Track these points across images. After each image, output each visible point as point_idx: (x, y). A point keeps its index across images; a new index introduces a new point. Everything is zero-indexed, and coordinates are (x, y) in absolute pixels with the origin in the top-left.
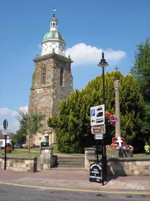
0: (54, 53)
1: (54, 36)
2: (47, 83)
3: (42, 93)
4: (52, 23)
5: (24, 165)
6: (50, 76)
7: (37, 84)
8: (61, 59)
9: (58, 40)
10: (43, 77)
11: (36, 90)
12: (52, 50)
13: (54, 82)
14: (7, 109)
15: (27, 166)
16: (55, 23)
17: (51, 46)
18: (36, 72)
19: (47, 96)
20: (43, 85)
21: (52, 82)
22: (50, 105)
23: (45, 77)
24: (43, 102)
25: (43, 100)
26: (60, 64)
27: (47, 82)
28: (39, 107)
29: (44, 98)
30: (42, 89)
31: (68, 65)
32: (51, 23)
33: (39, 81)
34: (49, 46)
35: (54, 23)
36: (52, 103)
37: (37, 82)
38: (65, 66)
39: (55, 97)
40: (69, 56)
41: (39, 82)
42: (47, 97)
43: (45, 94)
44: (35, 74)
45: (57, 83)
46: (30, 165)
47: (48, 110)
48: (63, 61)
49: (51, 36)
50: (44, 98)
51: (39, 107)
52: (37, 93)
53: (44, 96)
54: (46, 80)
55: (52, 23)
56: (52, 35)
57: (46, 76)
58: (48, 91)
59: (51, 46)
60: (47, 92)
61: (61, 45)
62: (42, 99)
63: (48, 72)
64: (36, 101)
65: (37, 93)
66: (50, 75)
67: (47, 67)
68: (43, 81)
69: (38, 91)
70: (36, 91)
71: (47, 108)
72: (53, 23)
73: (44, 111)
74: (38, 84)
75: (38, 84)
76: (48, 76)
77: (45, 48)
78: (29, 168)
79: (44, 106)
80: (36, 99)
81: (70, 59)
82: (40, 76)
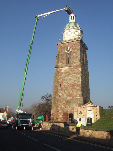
3: (68, 72)
4: (71, 17)
6: (77, 57)
7: (61, 64)
10: (68, 58)
11: (60, 69)
14: (81, 71)
17: (74, 33)
18: (60, 54)
19: (74, 74)
20: (69, 64)
22: (78, 82)
24: (70, 79)
25: (69, 77)
27: (73, 62)
29: (71, 76)
30: (68, 68)
32: (70, 16)
33: (64, 61)
34: (73, 33)
35: (73, 17)
37: (62, 62)
41: (64, 62)
42: (74, 75)
43: (71, 73)
44: (59, 55)
47: (76, 86)
50: (70, 76)
52: (62, 71)
53: (71, 74)
54: (72, 61)
55: (71, 17)
57: (72, 57)
58: (76, 70)
59: (74, 33)
63: (75, 53)
64: (61, 78)
65: (62, 71)
66: (77, 56)
68: (67, 61)
69: (63, 69)
70: (61, 70)
71: (75, 84)
73: (71, 88)
75: (63, 63)
77: (68, 35)
79: (71, 82)
80: (61, 77)
82: (64, 57)
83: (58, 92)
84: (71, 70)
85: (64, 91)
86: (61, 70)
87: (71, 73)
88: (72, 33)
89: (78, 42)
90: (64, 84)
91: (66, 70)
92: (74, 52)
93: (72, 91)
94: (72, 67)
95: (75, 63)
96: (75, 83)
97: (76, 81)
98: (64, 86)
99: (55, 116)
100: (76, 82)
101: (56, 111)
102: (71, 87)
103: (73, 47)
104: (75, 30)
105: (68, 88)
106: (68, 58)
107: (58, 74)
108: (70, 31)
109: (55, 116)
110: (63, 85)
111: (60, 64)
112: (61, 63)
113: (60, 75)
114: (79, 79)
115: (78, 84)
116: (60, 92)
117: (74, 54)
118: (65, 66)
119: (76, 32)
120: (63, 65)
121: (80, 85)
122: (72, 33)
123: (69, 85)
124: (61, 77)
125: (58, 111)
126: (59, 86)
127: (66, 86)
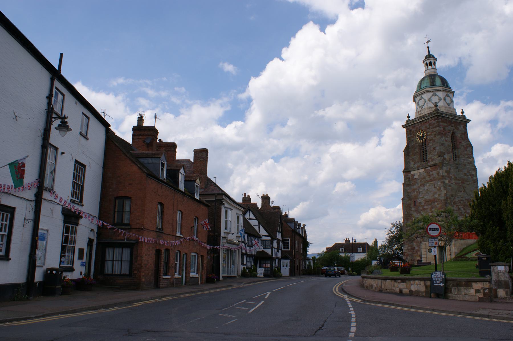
0: (438, 110)
1: (433, 84)
2: (430, 160)
3: (424, 178)
5: (472, 291)
7: (412, 163)
8: (450, 119)
9: (441, 88)
10: (423, 152)
11: (412, 173)
12: (433, 105)
13: (442, 158)
15: (477, 291)
16: (432, 61)
17: (430, 100)
21: (439, 158)
22: (439, 195)
23: (426, 151)
24: (427, 191)
25: (426, 188)
26: (450, 128)
27: (431, 158)
28: (420, 200)
30: (423, 170)
31: (462, 126)
33: (417, 158)
36: (444, 192)
38: (458, 129)
39: (447, 181)
40: (463, 112)
43: (429, 179)
45: (448, 159)
46: (482, 291)
47: (436, 203)
48: (454, 122)
49: (428, 84)
50: (428, 185)
51: (420, 200)
52: (415, 177)
53: (428, 181)
54: (429, 156)
56: (430, 82)
58: (434, 173)
60: (433, 174)
61: (447, 95)
62: (424, 186)
64: (414, 190)
65: (415, 177)
67: (428, 134)
69: (416, 173)
70: (414, 175)
72: (428, 62)
73: (429, 206)
74: (415, 163)
75: (415, 163)
76: (432, 149)
78: (481, 295)
79: (429, 197)
80: (414, 187)
81: (464, 117)
82: (417, 150)
83: (412, 215)
84: (428, 172)
85: (420, 213)
86: (414, 175)
87: (428, 178)
88: (425, 102)
89: (435, 120)
90: (420, 199)
91: (420, 174)
92: (430, 140)
93: (432, 212)
94: (429, 168)
95: (433, 160)
96: (435, 198)
97: (436, 193)
98: (420, 203)
99: (408, 257)
100: (436, 196)
101: (410, 248)
102: (430, 204)
103: (428, 130)
104: (431, 94)
105: (425, 207)
106: (423, 152)
107: (408, 183)
108: (422, 98)
109: (408, 257)
110: (418, 201)
111: (412, 164)
112: (413, 161)
113: (413, 185)
114: (440, 189)
115: (439, 199)
116: (414, 215)
117: (430, 142)
118: (418, 168)
119: (433, 98)
120: (416, 166)
121: (442, 200)
122: (425, 102)
123: (427, 202)
124: (414, 187)
125: (414, 249)
126: (412, 205)
127: (423, 204)
